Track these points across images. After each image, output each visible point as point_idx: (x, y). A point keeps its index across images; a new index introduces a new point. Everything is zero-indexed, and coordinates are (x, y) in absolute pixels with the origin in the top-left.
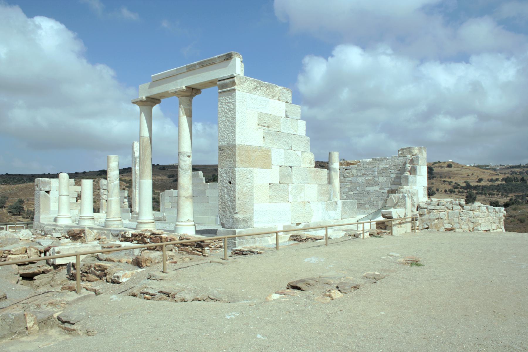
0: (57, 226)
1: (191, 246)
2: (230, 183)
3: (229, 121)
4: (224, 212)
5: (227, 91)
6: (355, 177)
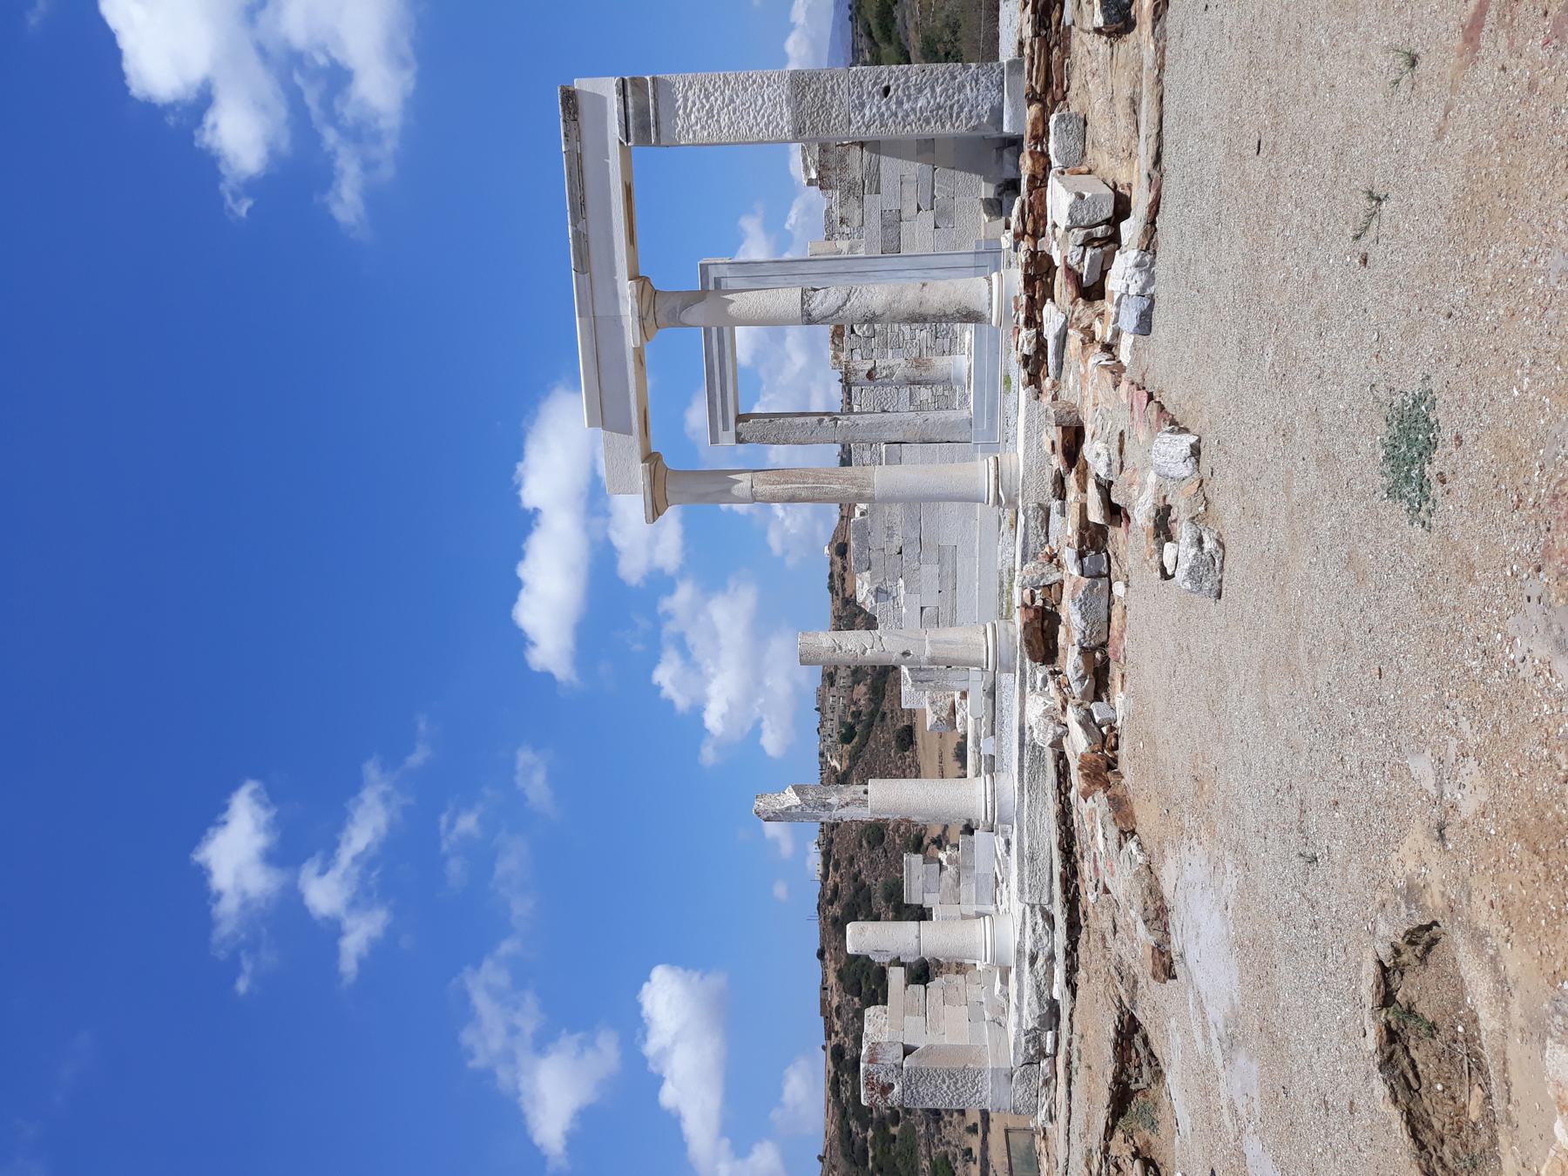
0: (1020, 952)
1: (1049, 52)
2: (887, 90)
3: (732, 101)
4: (961, 108)
5: (656, 110)
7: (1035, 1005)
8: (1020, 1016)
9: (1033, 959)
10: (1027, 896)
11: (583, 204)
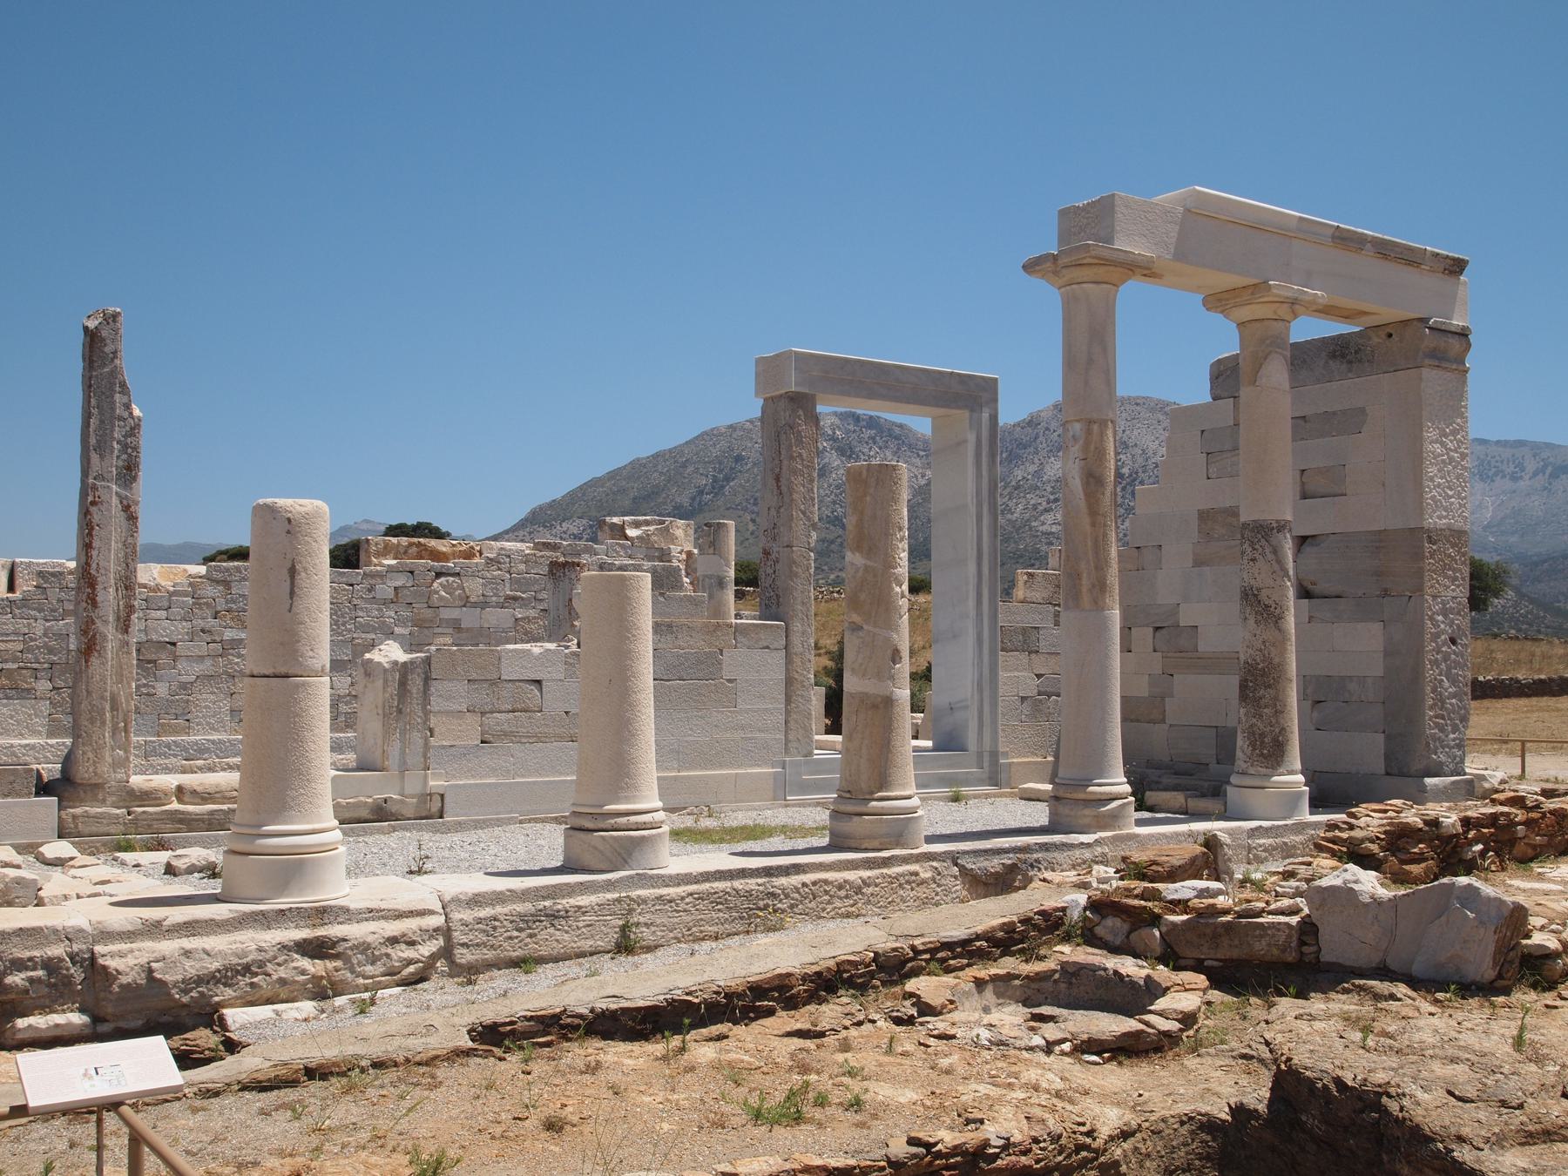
0: (322, 914)
2: (1453, 641)
6: (475, 605)
7: (191, 968)
8: (129, 935)
9: (317, 949)
10: (467, 915)
11: (1385, 256)
